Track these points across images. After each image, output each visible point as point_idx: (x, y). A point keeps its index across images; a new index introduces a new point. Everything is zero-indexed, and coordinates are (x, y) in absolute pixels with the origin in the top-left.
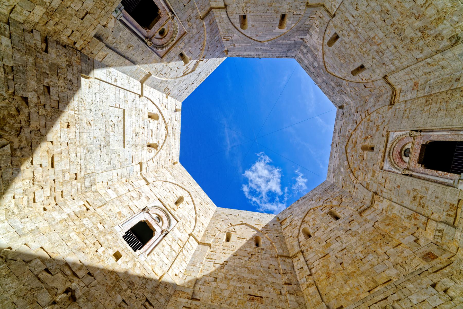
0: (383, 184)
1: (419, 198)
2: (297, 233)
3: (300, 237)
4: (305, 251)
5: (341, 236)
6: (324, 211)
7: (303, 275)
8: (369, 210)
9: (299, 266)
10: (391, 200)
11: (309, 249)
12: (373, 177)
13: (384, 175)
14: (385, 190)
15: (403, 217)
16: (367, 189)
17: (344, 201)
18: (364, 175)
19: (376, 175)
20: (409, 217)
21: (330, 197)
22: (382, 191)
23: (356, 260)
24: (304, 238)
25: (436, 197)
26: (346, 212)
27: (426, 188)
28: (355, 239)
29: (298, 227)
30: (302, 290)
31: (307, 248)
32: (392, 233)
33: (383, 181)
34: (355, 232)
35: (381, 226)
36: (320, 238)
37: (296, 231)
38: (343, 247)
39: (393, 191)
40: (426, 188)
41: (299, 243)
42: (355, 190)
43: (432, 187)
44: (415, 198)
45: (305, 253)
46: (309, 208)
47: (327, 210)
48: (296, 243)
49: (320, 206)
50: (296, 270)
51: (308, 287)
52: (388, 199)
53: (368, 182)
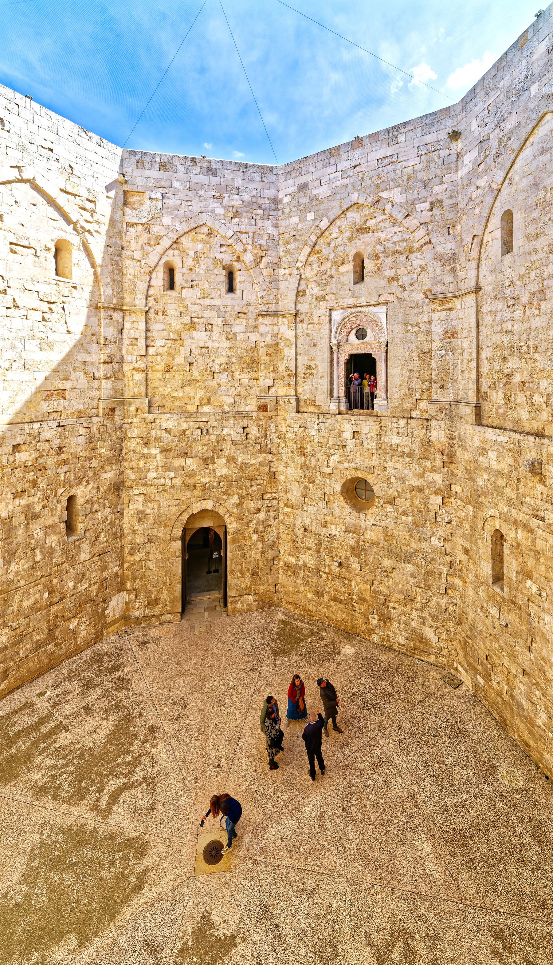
0: (311, 321)
1: (310, 372)
2: (153, 265)
3: (154, 275)
4: (152, 311)
5: (214, 327)
6: (222, 256)
7: (133, 350)
8: (271, 318)
9: (133, 334)
10: (296, 339)
11: (160, 313)
12: (317, 299)
13: (323, 317)
14: (305, 325)
15: (285, 362)
16: (297, 295)
17: (262, 266)
18: (315, 278)
19: (321, 303)
20: (288, 369)
21: (251, 235)
22: (302, 321)
23: (209, 370)
24: (161, 283)
25: (317, 388)
26: (249, 288)
27: (323, 376)
28: (226, 344)
29: (160, 249)
30: (124, 371)
31: (157, 308)
32: (262, 367)
33: (316, 319)
34: (235, 334)
35: (262, 351)
36: (185, 307)
37: (153, 259)
38: (207, 345)
39: (307, 338)
40: (323, 376)
41: (149, 286)
42: (288, 271)
43: (325, 382)
44: (309, 367)
45: (151, 315)
46: (204, 218)
47: (227, 258)
48: (142, 286)
49: (224, 237)
50: (125, 336)
51: (134, 369)
52: (296, 334)
53: (307, 293)
